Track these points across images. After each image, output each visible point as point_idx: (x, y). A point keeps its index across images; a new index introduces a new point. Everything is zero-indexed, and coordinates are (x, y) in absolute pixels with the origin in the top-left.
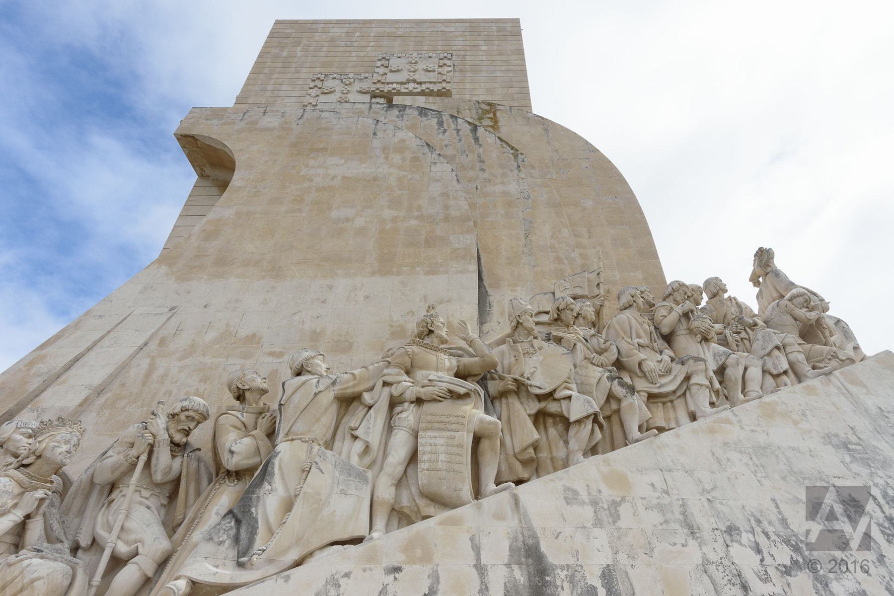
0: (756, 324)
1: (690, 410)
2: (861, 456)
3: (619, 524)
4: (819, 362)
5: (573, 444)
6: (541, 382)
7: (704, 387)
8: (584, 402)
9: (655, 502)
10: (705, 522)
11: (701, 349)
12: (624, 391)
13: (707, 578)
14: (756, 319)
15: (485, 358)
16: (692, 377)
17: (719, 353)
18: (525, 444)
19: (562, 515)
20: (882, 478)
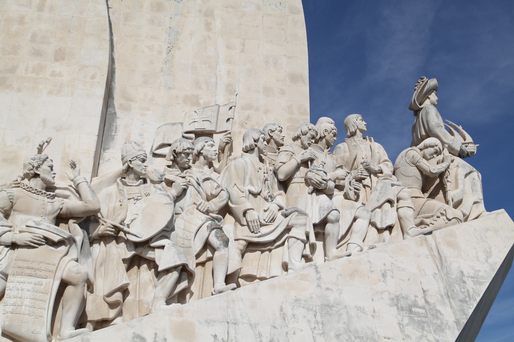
0: (381, 172)
1: (283, 261)
2: (420, 319)
7: (299, 241)
8: (174, 254)
11: (310, 201)
12: (218, 242)
14: (381, 165)
16: (292, 229)
17: (324, 207)
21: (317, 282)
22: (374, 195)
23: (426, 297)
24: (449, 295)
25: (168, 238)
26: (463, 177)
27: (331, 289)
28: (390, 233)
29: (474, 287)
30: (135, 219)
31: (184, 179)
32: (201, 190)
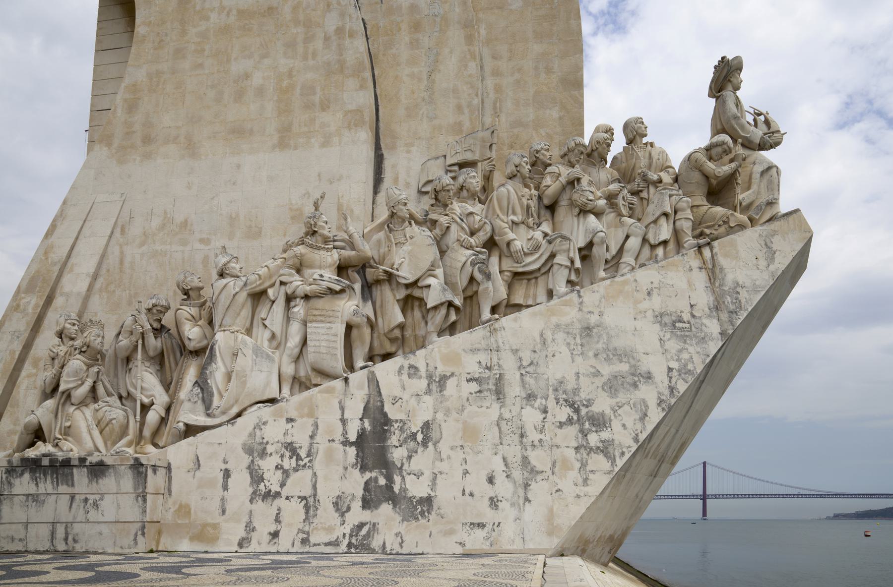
0: (660, 181)
2: (683, 333)
3: (445, 392)
4: (708, 227)
5: (431, 327)
6: (406, 274)
7: (563, 267)
9: (477, 376)
10: (514, 390)
12: (481, 276)
13: (498, 429)
14: (662, 174)
15: (361, 253)
18: (392, 326)
19: (404, 386)
20: (690, 353)
21: (579, 306)
22: (651, 208)
23: (693, 312)
24: (717, 307)
25: (434, 276)
26: (758, 175)
27: (593, 313)
28: (665, 248)
29: (747, 297)
30: (402, 262)
31: (446, 217)
32: (464, 225)
